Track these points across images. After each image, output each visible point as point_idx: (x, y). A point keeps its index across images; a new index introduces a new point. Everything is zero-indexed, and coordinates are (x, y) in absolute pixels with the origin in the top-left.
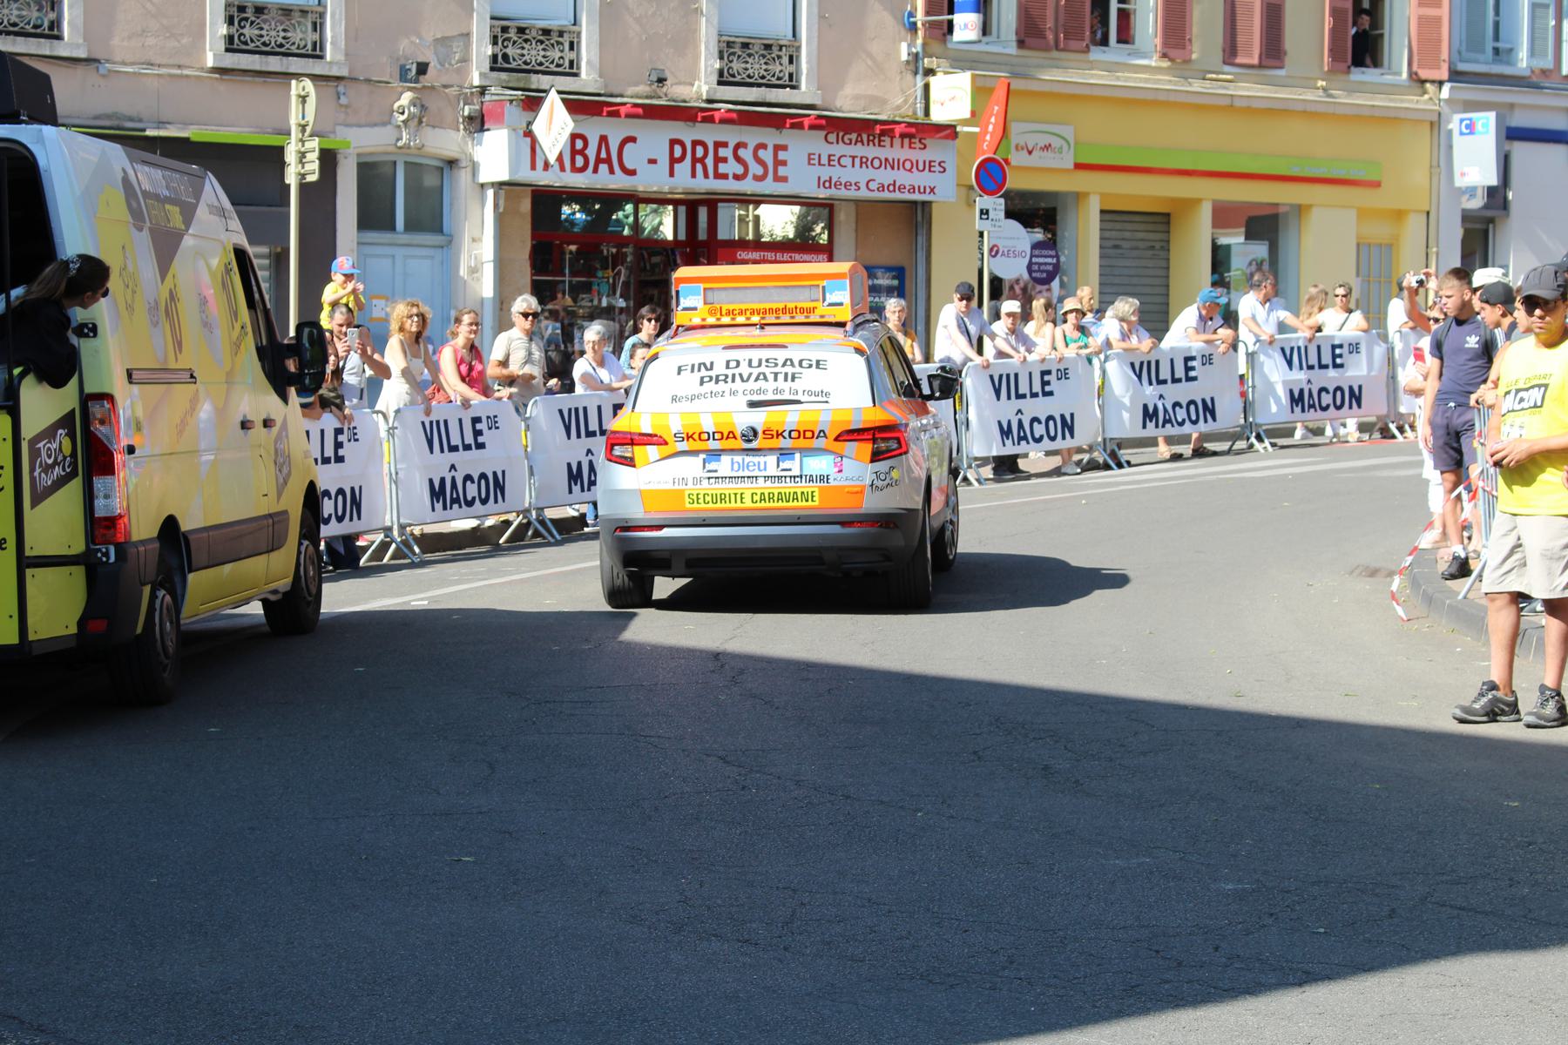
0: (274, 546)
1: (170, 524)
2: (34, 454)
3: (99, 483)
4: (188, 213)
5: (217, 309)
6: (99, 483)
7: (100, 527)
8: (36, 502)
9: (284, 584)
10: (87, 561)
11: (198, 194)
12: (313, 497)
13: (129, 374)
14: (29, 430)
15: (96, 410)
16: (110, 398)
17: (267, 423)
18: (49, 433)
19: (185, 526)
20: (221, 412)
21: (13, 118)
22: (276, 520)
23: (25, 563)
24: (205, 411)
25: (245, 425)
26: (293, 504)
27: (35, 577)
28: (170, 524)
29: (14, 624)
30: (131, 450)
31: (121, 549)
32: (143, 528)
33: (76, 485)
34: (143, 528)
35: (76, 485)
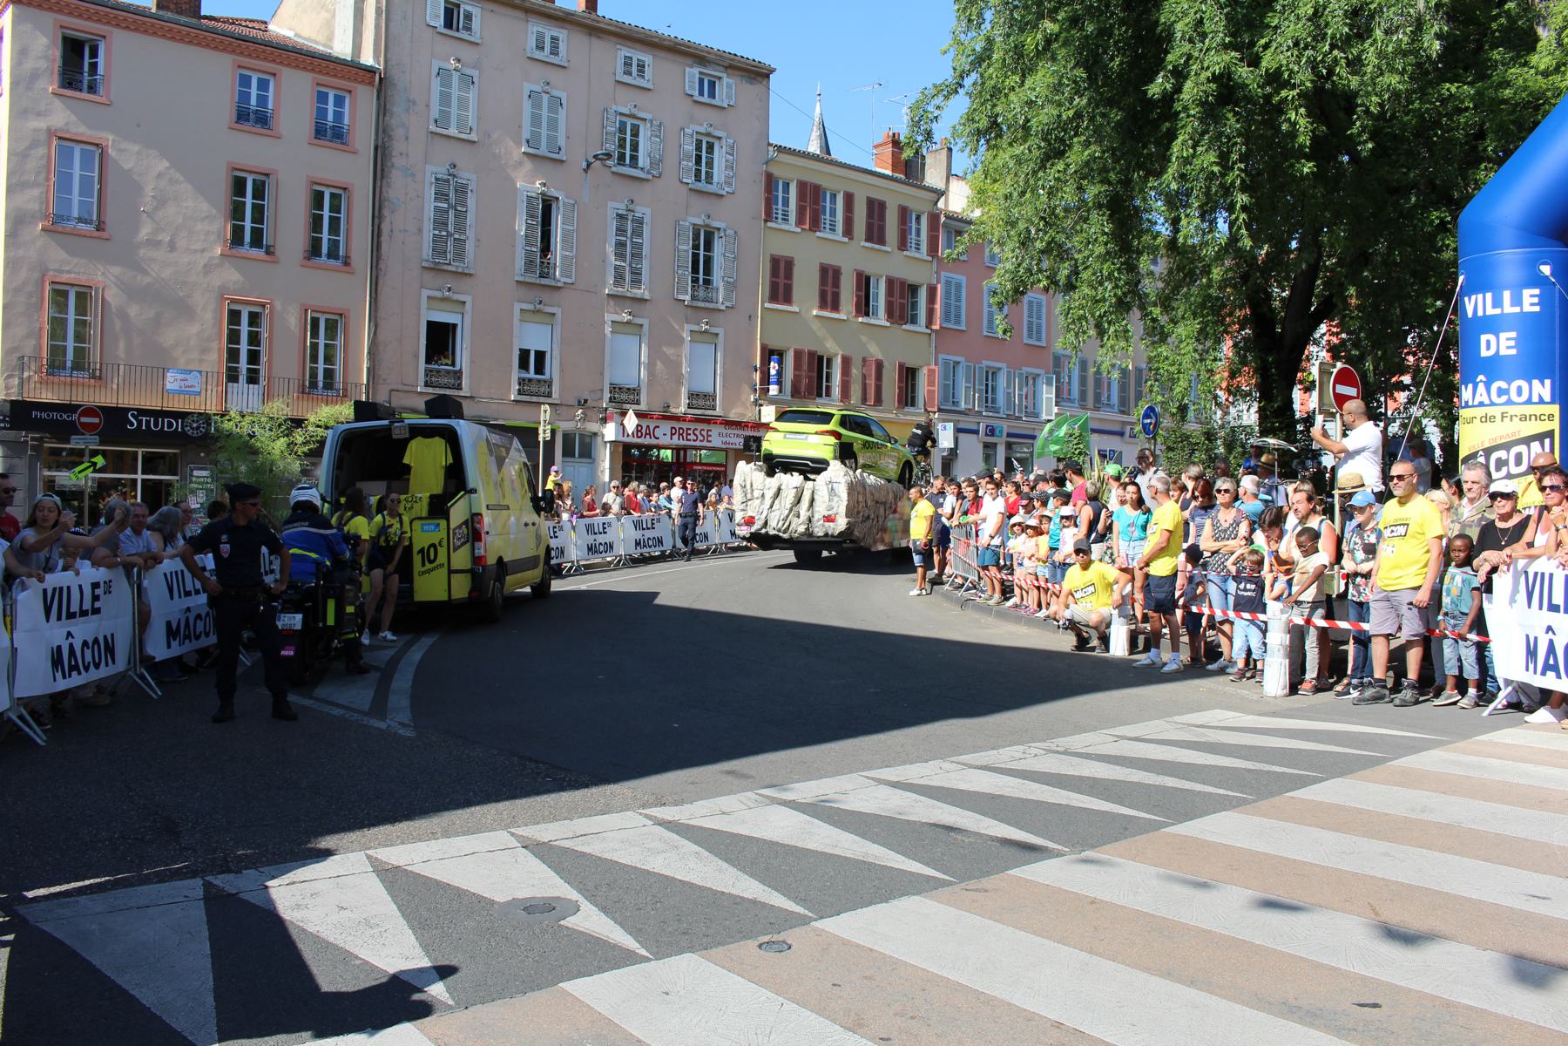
0: (535, 566)
1: (500, 559)
2: (454, 534)
3: (476, 544)
4: (508, 450)
5: (517, 484)
6: (476, 544)
7: (477, 560)
8: (455, 549)
9: (538, 580)
10: (471, 571)
11: (511, 444)
12: (548, 550)
13: (487, 506)
14: (453, 526)
15: (476, 518)
16: (480, 515)
17: (534, 524)
18: (460, 527)
19: (506, 559)
20: (518, 520)
21: (449, 417)
22: (537, 558)
23: (450, 572)
24: (512, 519)
25: (526, 525)
26: (542, 553)
27: (454, 577)
28: (500, 559)
29: (447, 594)
30: (488, 533)
31: (484, 567)
32: (491, 560)
33: (468, 546)
34: (491, 560)
35: (468, 546)
